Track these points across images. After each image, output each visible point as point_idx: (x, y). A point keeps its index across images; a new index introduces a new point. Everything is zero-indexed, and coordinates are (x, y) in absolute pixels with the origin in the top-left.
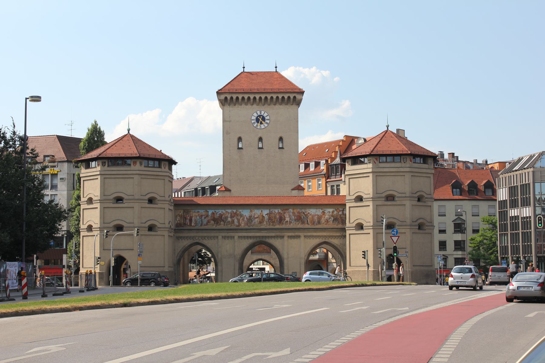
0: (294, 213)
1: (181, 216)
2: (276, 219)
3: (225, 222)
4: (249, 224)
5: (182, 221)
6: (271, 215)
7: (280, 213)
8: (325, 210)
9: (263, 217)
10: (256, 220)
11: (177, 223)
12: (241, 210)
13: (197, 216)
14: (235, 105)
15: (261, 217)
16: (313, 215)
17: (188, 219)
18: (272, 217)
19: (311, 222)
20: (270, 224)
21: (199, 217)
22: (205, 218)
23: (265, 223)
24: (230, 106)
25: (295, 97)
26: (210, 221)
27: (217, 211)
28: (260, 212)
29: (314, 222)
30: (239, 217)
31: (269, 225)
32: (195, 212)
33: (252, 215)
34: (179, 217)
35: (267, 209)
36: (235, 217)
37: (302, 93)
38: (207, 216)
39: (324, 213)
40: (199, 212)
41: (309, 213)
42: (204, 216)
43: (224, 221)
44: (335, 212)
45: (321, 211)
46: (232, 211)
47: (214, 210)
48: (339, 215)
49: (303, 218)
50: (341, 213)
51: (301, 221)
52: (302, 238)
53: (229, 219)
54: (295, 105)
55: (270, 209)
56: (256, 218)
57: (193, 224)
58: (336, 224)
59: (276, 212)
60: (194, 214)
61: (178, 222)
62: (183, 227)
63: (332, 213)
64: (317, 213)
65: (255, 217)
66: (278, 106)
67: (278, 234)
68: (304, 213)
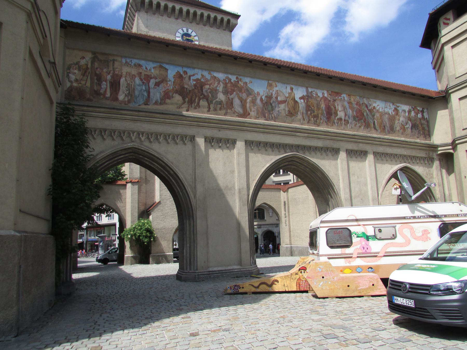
0: (350, 103)
1: (85, 71)
2: (320, 112)
3: (212, 102)
4: (267, 115)
5: (88, 84)
6: (310, 100)
7: (326, 97)
8: (398, 107)
9: (296, 102)
10: (282, 106)
11: (71, 87)
12: (247, 80)
13: (133, 77)
14: (154, 14)
15: (292, 103)
16: (381, 113)
17: (106, 81)
18: (313, 106)
19: (380, 127)
20: (309, 120)
21: (141, 80)
22: (157, 84)
23: (299, 116)
24: (148, 14)
25: (229, 21)
26: (171, 94)
27: (190, 72)
28: (289, 90)
29: (384, 126)
30: (244, 95)
31: (308, 122)
32: (127, 64)
33: (272, 94)
34: (76, 71)
35: (302, 86)
36: (235, 93)
37: (237, 17)
38: (164, 80)
39: (396, 110)
40: (140, 66)
41: (374, 108)
42: (156, 79)
43: (207, 100)
44: (413, 114)
45: (393, 107)
46: (227, 78)
47: (183, 67)
48: (419, 120)
49: (366, 117)
50: (421, 116)
51: (364, 122)
52: (370, 157)
53: (221, 97)
54: (228, 31)
55: (307, 88)
56: (282, 102)
57: (121, 97)
58: (416, 136)
59: (319, 96)
60: (125, 70)
61: (75, 84)
62: (89, 100)
63: (409, 114)
64: (386, 110)
65: (279, 99)
66: (207, 28)
67: (328, 144)
68: (367, 107)
